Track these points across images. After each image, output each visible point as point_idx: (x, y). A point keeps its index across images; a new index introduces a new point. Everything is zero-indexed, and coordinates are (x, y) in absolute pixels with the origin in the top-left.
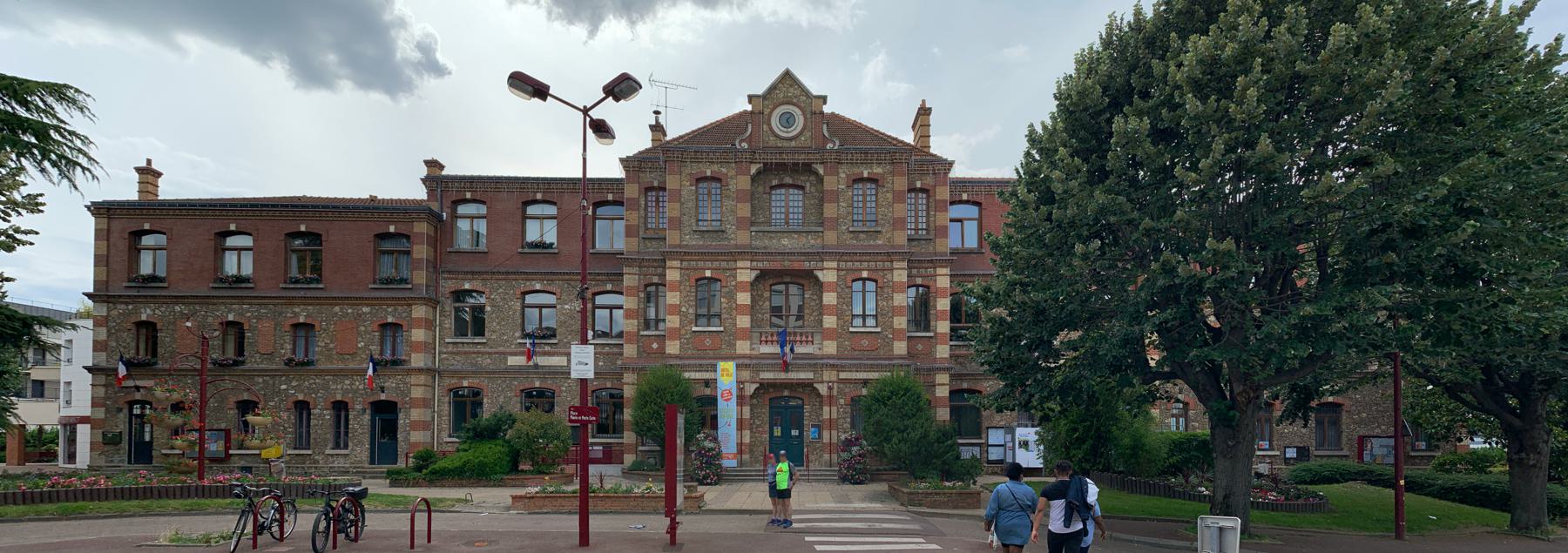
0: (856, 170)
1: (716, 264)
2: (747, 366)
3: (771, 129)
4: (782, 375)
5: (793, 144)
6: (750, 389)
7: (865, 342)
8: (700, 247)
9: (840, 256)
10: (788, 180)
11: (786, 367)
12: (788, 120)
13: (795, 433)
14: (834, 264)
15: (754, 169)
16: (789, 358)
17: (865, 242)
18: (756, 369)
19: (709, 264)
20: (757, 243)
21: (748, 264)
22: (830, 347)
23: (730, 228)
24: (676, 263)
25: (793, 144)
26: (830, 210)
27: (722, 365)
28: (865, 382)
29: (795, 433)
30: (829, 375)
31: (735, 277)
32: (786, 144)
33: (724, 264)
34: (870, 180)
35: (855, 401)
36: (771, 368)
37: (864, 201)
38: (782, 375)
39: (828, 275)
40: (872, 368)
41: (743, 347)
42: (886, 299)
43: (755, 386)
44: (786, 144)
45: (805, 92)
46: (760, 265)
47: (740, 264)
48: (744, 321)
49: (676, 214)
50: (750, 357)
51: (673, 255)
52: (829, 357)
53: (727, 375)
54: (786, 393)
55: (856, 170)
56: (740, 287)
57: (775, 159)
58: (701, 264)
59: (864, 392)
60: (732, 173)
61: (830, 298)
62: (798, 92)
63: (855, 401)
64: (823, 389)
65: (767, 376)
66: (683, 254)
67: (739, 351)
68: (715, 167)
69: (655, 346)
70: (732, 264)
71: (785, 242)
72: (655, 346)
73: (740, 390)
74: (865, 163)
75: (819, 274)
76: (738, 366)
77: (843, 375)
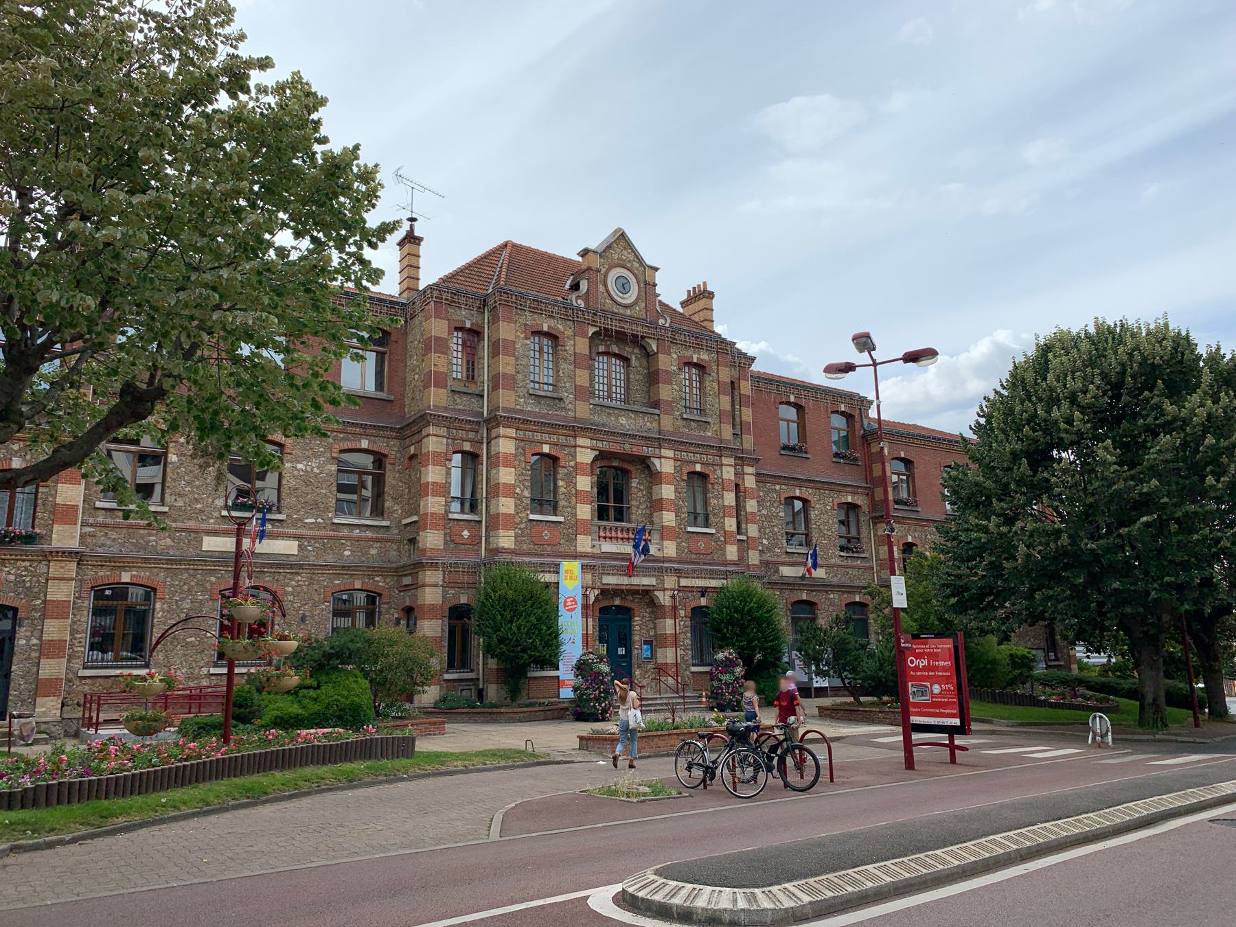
0: (687, 353)
1: (554, 438)
2: (592, 567)
3: (607, 291)
4: (625, 580)
5: (628, 312)
6: (592, 596)
7: (701, 545)
8: (535, 414)
9: (677, 444)
10: (615, 349)
11: (631, 570)
12: (624, 287)
13: (621, 651)
14: (670, 453)
15: (591, 330)
16: (639, 560)
17: (694, 433)
18: (605, 571)
19: (546, 437)
20: (596, 419)
21: (587, 442)
22: (670, 549)
23: (568, 397)
24: (511, 432)
25: (628, 312)
26: (665, 392)
27: (566, 565)
28: (703, 591)
29: (621, 651)
30: (670, 582)
31: (574, 456)
32: (621, 311)
33: (562, 440)
34: (696, 365)
35: (698, 613)
36: (615, 571)
37: (690, 386)
38: (625, 580)
39: (665, 464)
40: (712, 575)
41: (584, 543)
42: (716, 497)
43: (597, 592)
44: (621, 311)
45: (640, 261)
46: (600, 445)
47: (580, 441)
48: (585, 511)
49: (510, 370)
50: (593, 557)
51: (509, 421)
52: (670, 560)
53: (571, 580)
54: (617, 602)
55: (687, 353)
56: (577, 469)
57: (614, 326)
58: (538, 436)
59: (703, 602)
60: (569, 332)
61: (667, 491)
62: (631, 257)
63: (697, 612)
64: (664, 598)
65: (611, 580)
66: (519, 422)
67: (579, 549)
68: (552, 323)
69: (466, 533)
70: (571, 441)
71: (623, 420)
72: (466, 533)
73: (585, 596)
74: (698, 347)
75: (656, 462)
76: (584, 567)
77: (684, 582)
